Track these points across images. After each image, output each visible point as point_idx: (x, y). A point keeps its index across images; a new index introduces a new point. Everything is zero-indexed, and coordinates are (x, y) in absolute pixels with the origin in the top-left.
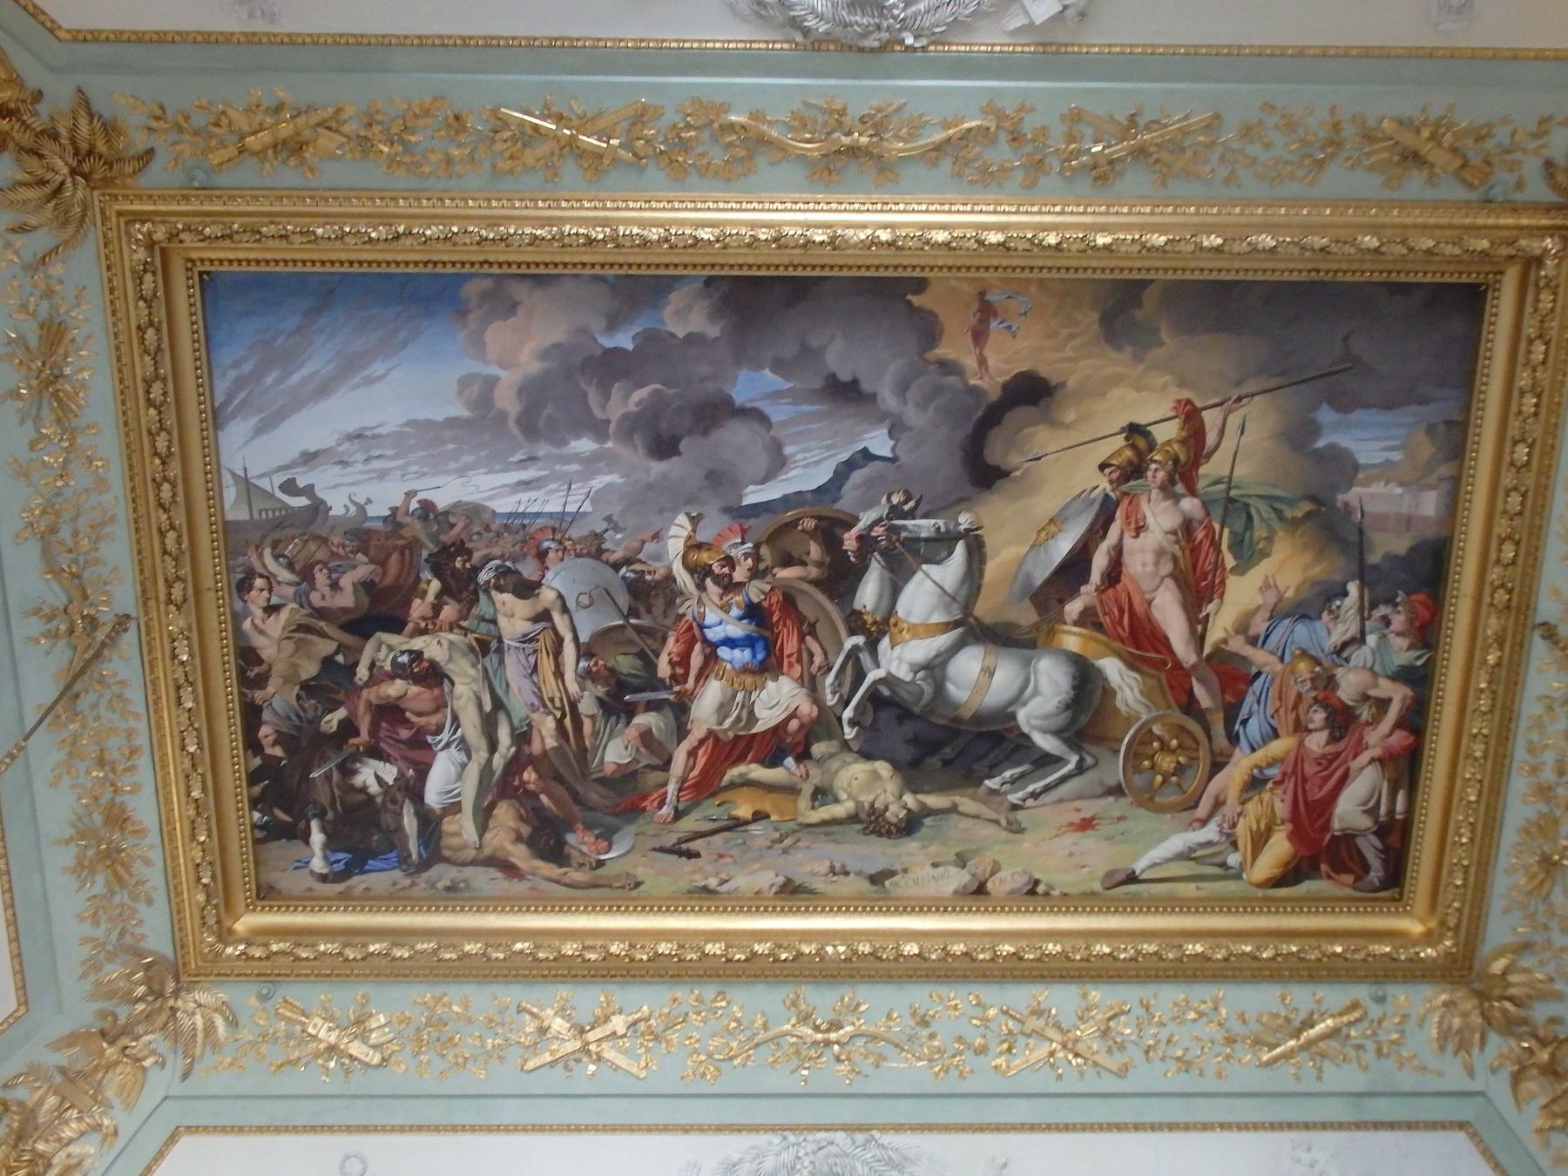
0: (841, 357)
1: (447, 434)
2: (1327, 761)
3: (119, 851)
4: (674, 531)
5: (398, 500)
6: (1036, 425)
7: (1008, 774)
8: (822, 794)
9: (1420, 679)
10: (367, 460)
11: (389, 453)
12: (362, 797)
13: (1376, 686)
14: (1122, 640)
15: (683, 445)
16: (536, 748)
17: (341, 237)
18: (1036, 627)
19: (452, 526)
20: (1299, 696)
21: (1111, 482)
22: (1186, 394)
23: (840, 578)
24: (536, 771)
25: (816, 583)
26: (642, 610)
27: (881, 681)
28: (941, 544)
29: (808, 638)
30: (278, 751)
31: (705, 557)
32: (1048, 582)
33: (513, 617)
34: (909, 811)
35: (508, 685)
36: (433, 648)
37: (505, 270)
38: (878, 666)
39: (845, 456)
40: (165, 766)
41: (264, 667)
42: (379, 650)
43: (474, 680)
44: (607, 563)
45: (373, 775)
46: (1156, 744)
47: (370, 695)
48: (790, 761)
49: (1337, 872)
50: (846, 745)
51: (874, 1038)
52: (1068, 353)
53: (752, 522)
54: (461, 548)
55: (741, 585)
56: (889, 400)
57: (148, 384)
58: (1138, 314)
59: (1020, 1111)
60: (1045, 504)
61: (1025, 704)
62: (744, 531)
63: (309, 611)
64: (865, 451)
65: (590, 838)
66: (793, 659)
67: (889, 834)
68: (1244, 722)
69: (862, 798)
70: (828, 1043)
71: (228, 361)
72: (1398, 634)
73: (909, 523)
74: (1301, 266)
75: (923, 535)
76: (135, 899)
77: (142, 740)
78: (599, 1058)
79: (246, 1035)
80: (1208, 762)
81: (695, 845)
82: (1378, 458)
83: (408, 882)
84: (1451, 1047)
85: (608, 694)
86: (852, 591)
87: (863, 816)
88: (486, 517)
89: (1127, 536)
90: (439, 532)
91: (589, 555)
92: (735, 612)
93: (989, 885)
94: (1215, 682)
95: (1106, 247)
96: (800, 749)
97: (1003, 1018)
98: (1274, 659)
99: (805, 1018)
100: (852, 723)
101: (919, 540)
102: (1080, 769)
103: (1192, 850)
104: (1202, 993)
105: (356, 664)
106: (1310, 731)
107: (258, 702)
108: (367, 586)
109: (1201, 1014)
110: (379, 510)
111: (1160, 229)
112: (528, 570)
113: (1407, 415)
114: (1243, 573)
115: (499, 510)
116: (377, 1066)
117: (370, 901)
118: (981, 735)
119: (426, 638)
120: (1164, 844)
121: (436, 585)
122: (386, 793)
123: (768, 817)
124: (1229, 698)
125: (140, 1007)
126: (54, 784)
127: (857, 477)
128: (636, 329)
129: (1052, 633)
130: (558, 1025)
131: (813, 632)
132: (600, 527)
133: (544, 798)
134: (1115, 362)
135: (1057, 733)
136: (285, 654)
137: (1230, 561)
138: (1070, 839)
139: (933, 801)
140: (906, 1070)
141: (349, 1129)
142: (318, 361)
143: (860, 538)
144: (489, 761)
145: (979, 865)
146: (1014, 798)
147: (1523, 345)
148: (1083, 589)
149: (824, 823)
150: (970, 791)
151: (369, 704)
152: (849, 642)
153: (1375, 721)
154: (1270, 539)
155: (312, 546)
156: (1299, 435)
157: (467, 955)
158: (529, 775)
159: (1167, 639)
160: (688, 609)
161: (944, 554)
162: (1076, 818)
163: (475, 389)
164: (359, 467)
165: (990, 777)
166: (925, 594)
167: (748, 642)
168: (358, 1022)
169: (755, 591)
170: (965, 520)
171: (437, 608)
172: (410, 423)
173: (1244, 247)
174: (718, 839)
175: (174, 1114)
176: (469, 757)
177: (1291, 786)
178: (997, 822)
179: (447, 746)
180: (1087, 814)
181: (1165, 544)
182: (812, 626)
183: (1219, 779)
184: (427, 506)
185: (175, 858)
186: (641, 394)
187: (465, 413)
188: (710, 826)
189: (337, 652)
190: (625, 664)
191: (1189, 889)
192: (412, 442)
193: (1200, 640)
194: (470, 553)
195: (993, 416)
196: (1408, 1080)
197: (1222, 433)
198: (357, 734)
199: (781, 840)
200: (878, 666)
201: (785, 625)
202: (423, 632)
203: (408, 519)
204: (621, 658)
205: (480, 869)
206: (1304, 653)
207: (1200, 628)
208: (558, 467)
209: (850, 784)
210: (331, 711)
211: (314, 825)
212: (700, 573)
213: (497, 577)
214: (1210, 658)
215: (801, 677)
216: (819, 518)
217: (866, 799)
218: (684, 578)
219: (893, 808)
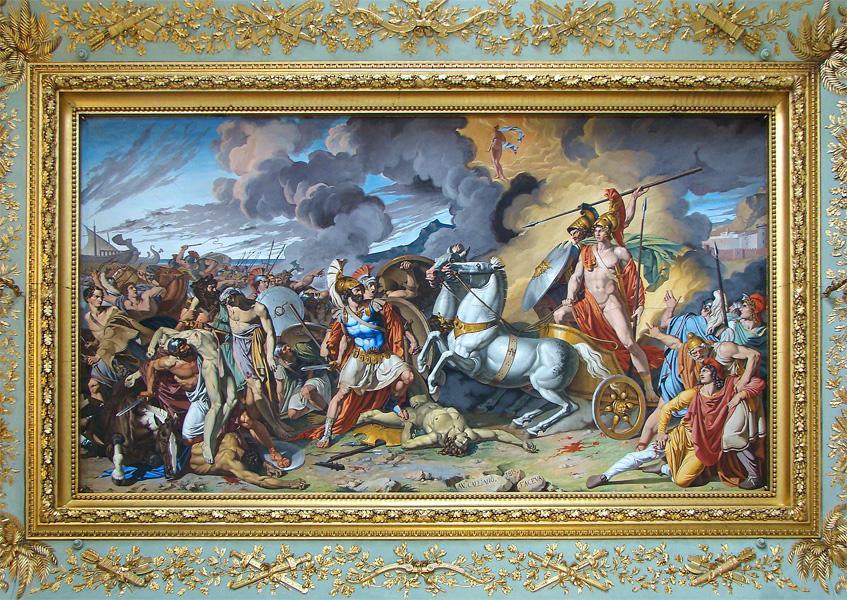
0: (422, 166)
1: (206, 213)
2: (715, 402)
4: (330, 270)
6: (530, 205)
7: (526, 415)
8: (417, 429)
9: (761, 344)
12: (146, 431)
13: (737, 352)
16: (249, 400)
18: (538, 325)
19: (207, 267)
22: (612, 186)
23: (425, 297)
26: (312, 317)
27: (450, 358)
28: (484, 275)
29: (407, 333)
30: (98, 397)
31: (348, 285)
33: (238, 319)
35: (234, 361)
36: (192, 337)
39: (426, 225)
41: (95, 342)
44: (292, 289)
45: (154, 416)
47: (155, 364)
48: (397, 408)
50: (430, 398)
54: (211, 280)
56: (449, 191)
58: (583, 139)
60: (539, 252)
61: (534, 371)
62: (370, 270)
65: (278, 457)
66: (398, 345)
67: (457, 454)
68: (663, 381)
72: (746, 319)
75: (471, 271)
80: (645, 406)
81: (340, 462)
82: (722, 219)
86: (432, 304)
87: (441, 443)
89: (586, 270)
90: (199, 270)
91: (282, 284)
92: (365, 317)
93: (519, 485)
96: (403, 400)
98: (676, 340)
100: (434, 384)
101: (468, 274)
102: (569, 412)
103: (640, 463)
105: (148, 345)
108: (155, 299)
110: (167, 256)
112: (248, 293)
118: (509, 390)
120: (623, 460)
121: (196, 301)
122: (160, 429)
127: (433, 237)
128: (310, 151)
129: (547, 328)
132: (289, 268)
133: (252, 432)
134: (572, 167)
135: (554, 389)
137: (646, 284)
139: (483, 433)
142: (139, 170)
143: (435, 273)
144: (222, 408)
145: (512, 474)
146: (530, 431)
147: (791, 162)
148: (564, 302)
149: (418, 447)
153: (739, 374)
155: (128, 274)
156: (677, 209)
158: (244, 417)
159: (614, 331)
160: (338, 315)
162: (569, 443)
163: (223, 187)
166: (472, 307)
167: (372, 335)
169: (377, 305)
170: (494, 261)
171: (196, 314)
172: (187, 207)
174: (355, 458)
176: (210, 407)
177: (695, 422)
178: (522, 446)
179: (197, 399)
182: (409, 325)
184: (193, 254)
186: (314, 188)
187: (217, 201)
190: (301, 348)
192: (187, 217)
193: (633, 331)
194: (216, 282)
195: (506, 200)
198: (146, 390)
201: (394, 324)
208: (266, 233)
209: (433, 423)
211: (117, 448)
212: (345, 294)
213: (230, 297)
214: (640, 340)
215: (404, 355)
216: (411, 261)
217: (443, 432)
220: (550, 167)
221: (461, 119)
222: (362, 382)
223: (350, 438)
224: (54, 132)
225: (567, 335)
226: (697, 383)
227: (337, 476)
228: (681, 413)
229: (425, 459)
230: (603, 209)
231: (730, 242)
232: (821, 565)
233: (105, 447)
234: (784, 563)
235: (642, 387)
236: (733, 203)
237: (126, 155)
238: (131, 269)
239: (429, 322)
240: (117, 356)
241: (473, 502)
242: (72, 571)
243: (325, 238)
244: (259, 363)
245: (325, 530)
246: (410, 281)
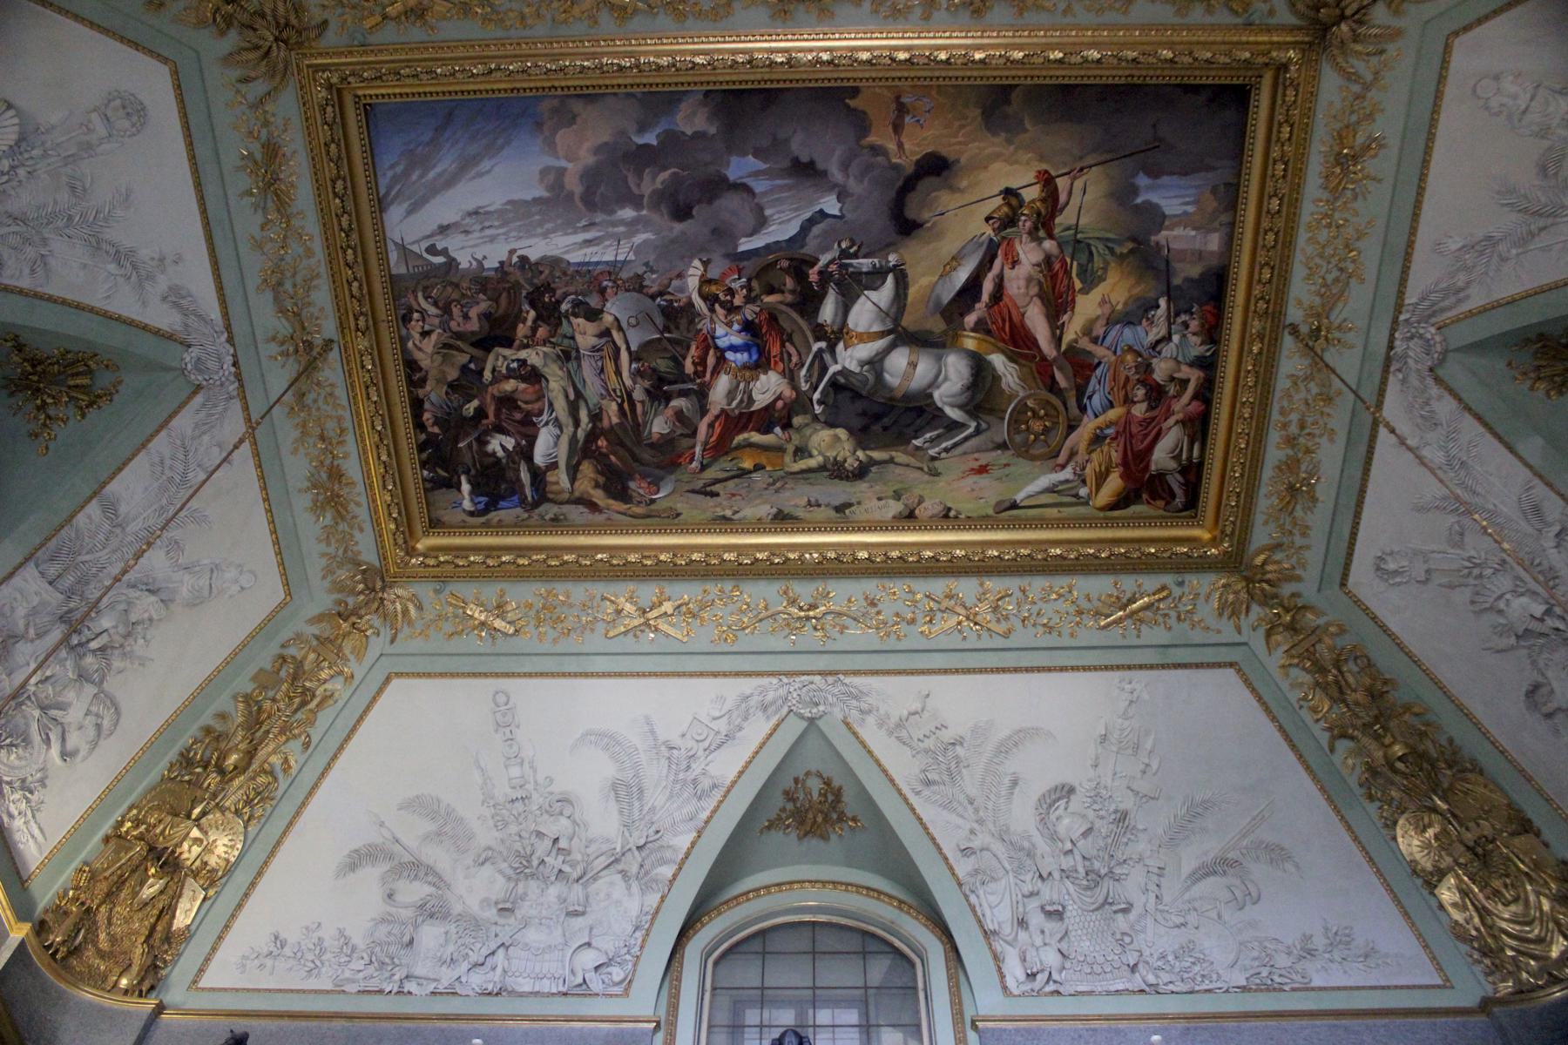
0: (800, 146)
2: (1147, 423)
3: (339, 496)
4: (691, 271)
7: (928, 436)
8: (801, 452)
9: (1208, 365)
12: (492, 459)
13: (1179, 371)
14: (1003, 341)
15: (694, 212)
16: (606, 423)
17: (453, 74)
18: (945, 333)
20: (1127, 378)
22: (1044, 166)
23: (808, 302)
25: (790, 305)
27: (839, 373)
28: (878, 275)
30: (436, 430)
31: (713, 288)
32: (953, 300)
33: (585, 334)
36: (533, 357)
37: (566, 92)
39: (808, 215)
40: (363, 440)
44: (647, 295)
45: (499, 444)
47: (494, 390)
48: (778, 430)
50: (816, 418)
51: (839, 614)
53: (745, 263)
54: (548, 287)
56: (837, 175)
57: (334, 182)
58: (1010, 110)
59: (938, 661)
60: (948, 247)
62: (740, 271)
64: (821, 211)
65: (644, 485)
67: (847, 478)
68: (1090, 398)
70: (808, 618)
71: (387, 164)
73: (854, 262)
74: (1120, 73)
76: (352, 528)
77: (348, 424)
78: (657, 629)
79: (429, 615)
81: (715, 488)
82: (1178, 210)
84: (1226, 615)
86: (817, 310)
92: (736, 327)
95: (982, 61)
97: (926, 601)
98: (1109, 353)
99: (793, 602)
100: (820, 402)
101: (861, 273)
103: (1055, 485)
104: (1061, 582)
108: (486, 316)
109: (1060, 596)
110: (491, 263)
111: (1020, 47)
112: (594, 301)
113: (1197, 180)
117: (500, 528)
120: (1037, 482)
121: (532, 314)
123: (763, 468)
125: (362, 597)
126: (295, 452)
127: (816, 230)
128: (658, 130)
129: (956, 337)
130: (629, 608)
131: (790, 340)
132: (640, 271)
133: (613, 458)
134: (993, 144)
135: (961, 407)
137: (1078, 285)
139: (877, 455)
140: (857, 635)
141: (497, 675)
142: (445, 163)
143: (820, 273)
144: (575, 433)
146: (932, 452)
149: (802, 471)
151: (493, 396)
152: (816, 346)
153: (1178, 396)
154: (1105, 269)
155: (449, 289)
156: (1123, 195)
157: (566, 563)
158: (602, 443)
160: (703, 325)
162: (976, 465)
163: (552, 177)
164: (477, 234)
166: (865, 313)
167: (745, 348)
168: (499, 607)
169: (749, 312)
170: (893, 259)
171: (534, 329)
172: (510, 202)
173: (1077, 59)
174: (731, 484)
175: (386, 666)
178: (921, 469)
180: (983, 462)
184: (524, 259)
185: (374, 501)
188: (726, 475)
190: (663, 365)
191: (1053, 512)
193: (1058, 340)
194: (554, 291)
196: (1198, 636)
197: (1070, 193)
198: (487, 417)
202: (526, 346)
206: (1130, 349)
211: (463, 479)
212: (711, 300)
216: (791, 259)
217: (831, 454)
218: (699, 303)
220: (965, 144)
222: (734, 403)
226: (1128, 401)
228: (1108, 431)
230: (1031, 194)
231: (1187, 238)
236: (1192, 191)
237: (428, 144)
238: (452, 283)
239: (813, 331)
240: (450, 385)
243: (684, 233)
244: (613, 382)
246: (789, 283)
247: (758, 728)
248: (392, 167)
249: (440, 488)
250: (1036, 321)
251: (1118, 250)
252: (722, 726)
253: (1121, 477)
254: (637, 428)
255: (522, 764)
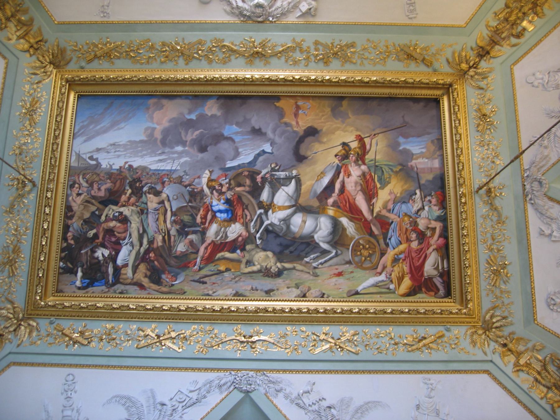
0: (256, 121)
1: (139, 145)
2: (419, 251)
4: (204, 175)
5: (122, 165)
7: (312, 256)
8: (249, 263)
9: (443, 219)
10: (115, 152)
11: (122, 150)
12: (97, 261)
14: (347, 211)
15: (208, 149)
16: (155, 245)
18: (319, 207)
19: (137, 173)
20: (407, 229)
21: (339, 160)
22: (358, 133)
23: (256, 191)
24: (154, 253)
25: (248, 192)
26: (193, 200)
28: (288, 179)
29: (246, 210)
30: (72, 242)
31: (213, 183)
33: (152, 202)
34: (279, 268)
36: (126, 211)
38: (268, 219)
39: (257, 152)
41: (73, 213)
42: (109, 210)
43: (138, 223)
44: (183, 185)
45: (101, 253)
46: (361, 247)
48: (238, 251)
49: (429, 291)
50: (257, 246)
52: (322, 120)
53: (228, 173)
55: (224, 193)
56: (270, 134)
58: (342, 109)
60: (319, 168)
61: (317, 233)
62: (226, 176)
63: (89, 196)
64: (263, 151)
65: (170, 277)
66: (240, 217)
67: (272, 277)
68: (390, 239)
69: (263, 264)
70: (248, 342)
72: (435, 205)
75: (282, 177)
81: (205, 280)
82: (419, 151)
83: (107, 290)
85: (180, 228)
86: (260, 195)
87: (263, 270)
88: (148, 170)
89: (345, 178)
90: (133, 175)
91: (178, 183)
92: (222, 201)
93: (307, 295)
94: (379, 226)
96: (242, 247)
100: (260, 238)
101: (280, 178)
105: (102, 215)
106: (412, 241)
107: (69, 224)
112: (159, 187)
113: (426, 138)
114: (383, 189)
115: (152, 168)
116: (87, 345)
118: (302, 243)
119: (125, 208)
121: (130, 191)
122: (104, 260)
123: (230, 270)
124: (384, 231)
127: (261, 158)
128: (197, 113)
133: (156, 262)
135: (328, 243)
136: (80, 210)
137: (378, 185)
138: (334, 279)
139: (287, 265)
142: (106, 123)
143: (262, 178)
144: (139, 250)
145: (303, 288)
146: (314, 265)
148: (333, 195)
149: (250, 273)
150: (300, 262)
151: (104, 228)
152: (259, 212)
153: (433, 235)
154: (390, 178)
155: (95, 176)
156: (394, 146)
158: (152, 255)
160: (208, 200)
161: (288, 183)
162: (336, 272)
163: (149, 131)
164: (112, 154)
165: (306, 257)
166: (282, 196)
167: (226, 211)
169: (229, 195)
170: (294, 172)
171: (129, 198)
172: (130, 141)
174: (213, 278)
175: (12, 358)
176: (133, 248)
177: (408, 262)
178: (309, 273)
179: (127, 244)
180: (340, 270)
181: (358, 180)
183: (384, 258)
184: (130, 166)
186: (197, 133)
187: (145, 139)
188: (211, 273)
189: (96, 210)
190: (186, 218)
192: (129, 147)
193: (372, 211)
194: (141, 181)
195: (301, 140)
196: (464, 357)
198: (98, 239)
199: (235, 278)
200: (268, 219)
202: (124, 206)
203: (124, 170)
204: (185, 216)
205: (132, 286)
207: (371, 207)
208: (171, 155)
210: (91, 230)
211: (80, 269)
212: (212, 188)
213: (149, 190)
214: (376, 217)
216: (249, 171)
217: (264, 264)
218: (207, 190)
219: (273, 268)
221: (278, 98)
223: (211, 268)
224: (63, 102)
225: (335, 213)
227: (202, 288)
229: (254, 279)
231: (425, 163)
232: (482, 341)
233: (73, 269)
234: (461, 339)
235: (378, 242)
238: (96, 173)
240: (85, 221)
241: (280, 303)
242: (48, 335)
244: (162, 226)
245: (194, 317)
246: (248, 182)
247: (214, 398)
248: (83, 122)
249: (67, 273)
250: (361, 202)
251: (395, 169)
252: (194, 396)
253: (410, 279)
254: (170, 248)
255: (73, 410)
